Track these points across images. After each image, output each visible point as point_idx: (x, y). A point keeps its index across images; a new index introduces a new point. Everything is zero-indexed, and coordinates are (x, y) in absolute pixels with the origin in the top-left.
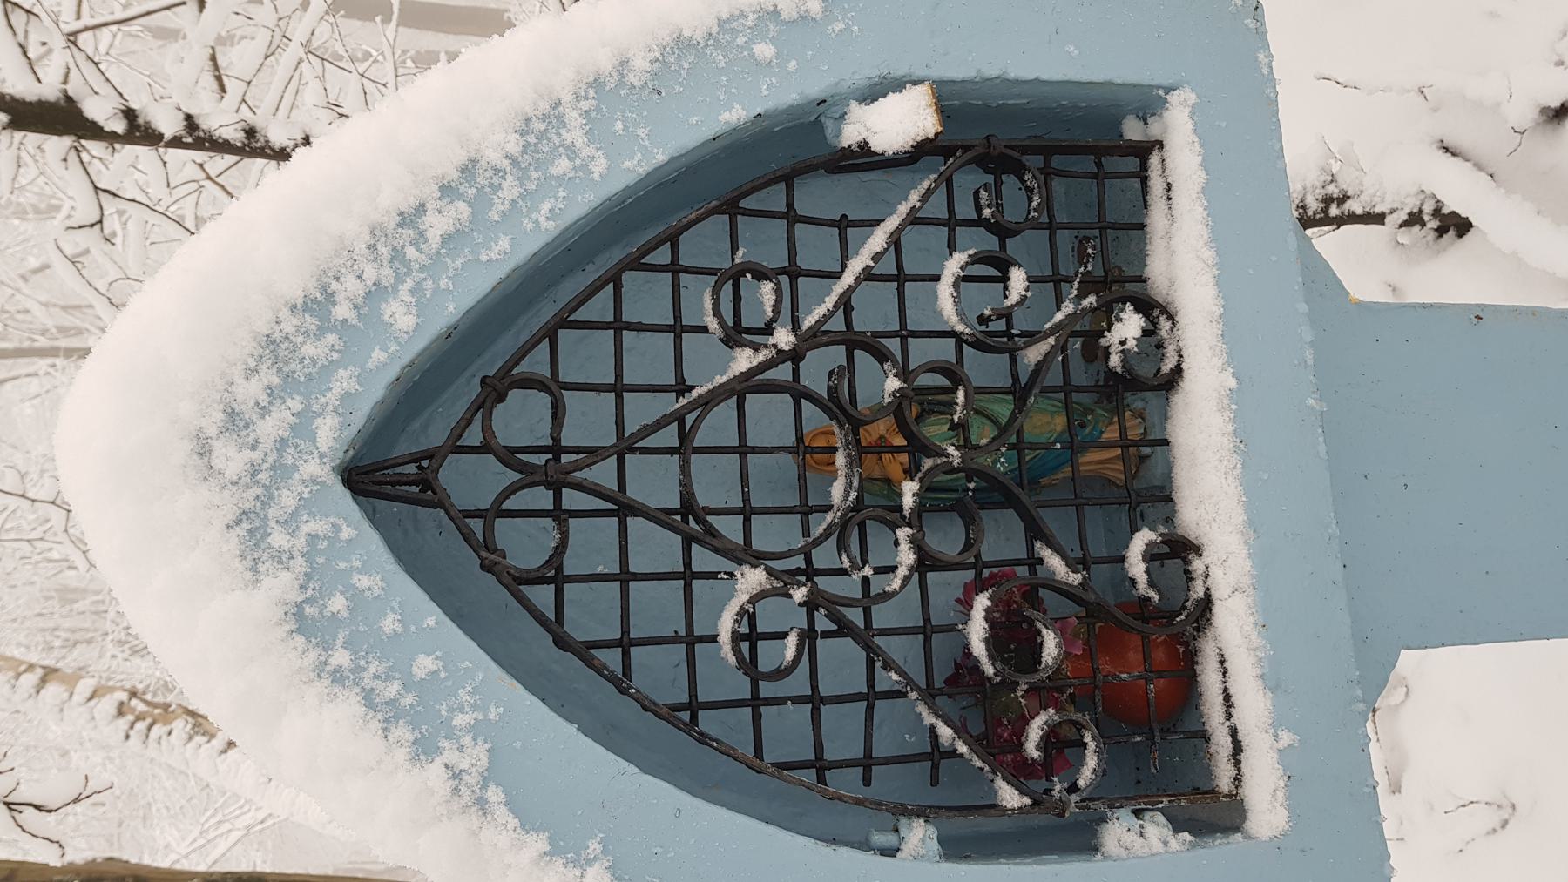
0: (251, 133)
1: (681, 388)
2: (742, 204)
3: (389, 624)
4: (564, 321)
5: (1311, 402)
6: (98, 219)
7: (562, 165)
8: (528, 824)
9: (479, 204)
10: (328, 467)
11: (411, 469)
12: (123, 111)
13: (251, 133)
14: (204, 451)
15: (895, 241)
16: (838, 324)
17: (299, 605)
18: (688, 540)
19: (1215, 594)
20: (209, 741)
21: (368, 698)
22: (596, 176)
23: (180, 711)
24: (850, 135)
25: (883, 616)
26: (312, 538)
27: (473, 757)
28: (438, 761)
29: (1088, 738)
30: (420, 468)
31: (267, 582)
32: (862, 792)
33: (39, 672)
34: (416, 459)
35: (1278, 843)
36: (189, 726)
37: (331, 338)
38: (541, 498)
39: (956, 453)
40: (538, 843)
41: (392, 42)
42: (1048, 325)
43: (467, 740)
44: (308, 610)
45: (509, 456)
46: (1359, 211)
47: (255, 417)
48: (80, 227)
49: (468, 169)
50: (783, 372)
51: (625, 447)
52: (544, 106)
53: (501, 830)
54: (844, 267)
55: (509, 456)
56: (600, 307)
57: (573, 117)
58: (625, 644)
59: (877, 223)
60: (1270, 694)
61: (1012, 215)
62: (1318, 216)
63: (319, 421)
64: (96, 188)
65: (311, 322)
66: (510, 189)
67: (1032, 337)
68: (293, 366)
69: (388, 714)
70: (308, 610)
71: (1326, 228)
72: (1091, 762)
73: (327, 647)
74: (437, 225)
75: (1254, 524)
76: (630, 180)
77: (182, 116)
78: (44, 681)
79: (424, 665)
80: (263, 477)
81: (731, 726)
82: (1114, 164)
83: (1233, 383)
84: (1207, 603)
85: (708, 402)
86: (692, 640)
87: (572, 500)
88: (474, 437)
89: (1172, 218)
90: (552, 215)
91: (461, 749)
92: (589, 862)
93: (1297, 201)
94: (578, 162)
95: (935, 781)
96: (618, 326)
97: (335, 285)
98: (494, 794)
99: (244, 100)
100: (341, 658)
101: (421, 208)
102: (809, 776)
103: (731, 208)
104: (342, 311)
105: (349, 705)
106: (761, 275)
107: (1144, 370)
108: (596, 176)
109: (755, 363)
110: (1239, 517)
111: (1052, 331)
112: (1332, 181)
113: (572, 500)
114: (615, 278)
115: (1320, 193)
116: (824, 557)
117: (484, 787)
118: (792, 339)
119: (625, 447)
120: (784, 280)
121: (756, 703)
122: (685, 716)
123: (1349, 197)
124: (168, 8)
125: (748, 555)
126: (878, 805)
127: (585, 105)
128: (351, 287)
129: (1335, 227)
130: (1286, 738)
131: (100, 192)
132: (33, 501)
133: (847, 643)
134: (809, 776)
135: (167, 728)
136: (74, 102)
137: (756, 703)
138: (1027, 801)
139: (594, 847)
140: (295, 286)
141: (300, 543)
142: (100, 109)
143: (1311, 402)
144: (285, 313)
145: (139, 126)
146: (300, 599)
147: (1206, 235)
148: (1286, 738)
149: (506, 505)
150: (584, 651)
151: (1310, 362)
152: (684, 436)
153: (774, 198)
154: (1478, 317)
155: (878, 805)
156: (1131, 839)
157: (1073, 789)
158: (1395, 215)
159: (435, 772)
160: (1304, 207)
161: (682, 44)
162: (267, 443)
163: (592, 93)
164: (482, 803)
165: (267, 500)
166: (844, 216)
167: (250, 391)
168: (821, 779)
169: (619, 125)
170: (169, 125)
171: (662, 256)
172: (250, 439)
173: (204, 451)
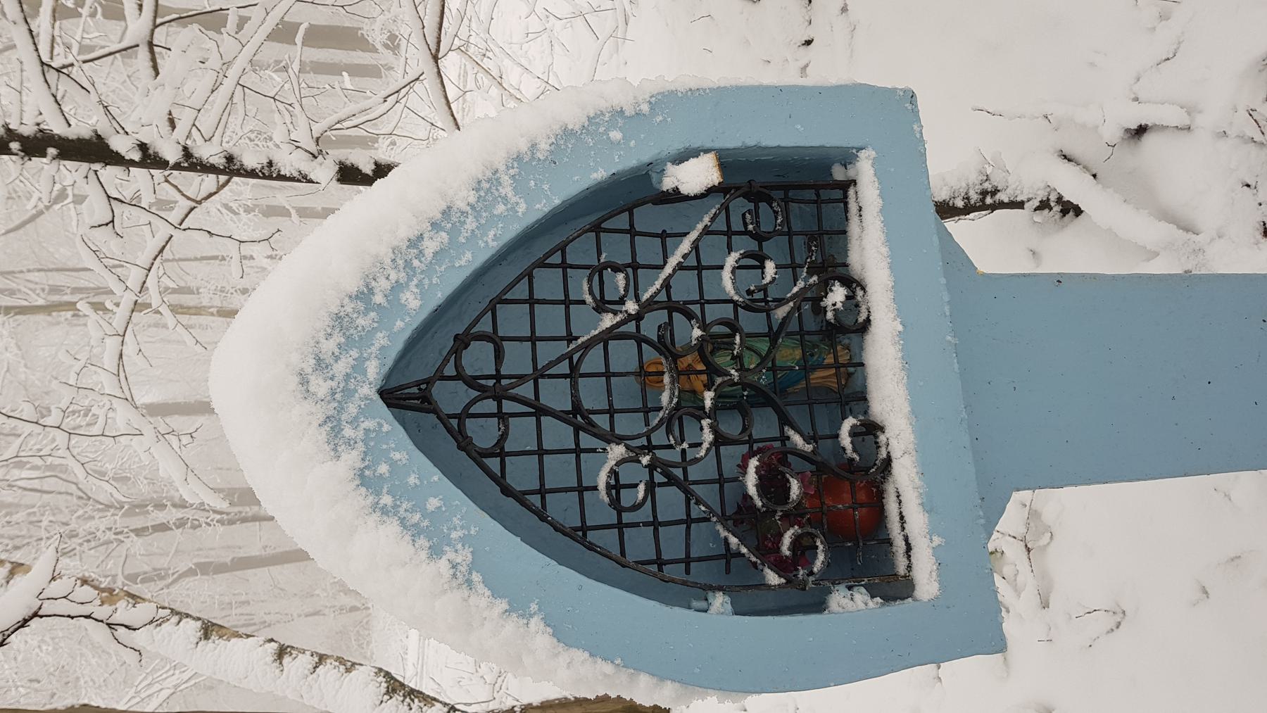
0: (230, 159)
1: (570, 338)
2: (603, 225)
3: (412, 480)
4: (501, 300)
5: (949, 338)
6: (111, 219)
7: (500, 209)
8: (496, 594)
9: (454, 232)
10: (374, 390)
11: (415, 390)
12: (138, 145)
13: (230, 159)
15: (696, 246)
16: (662, 297)
17: (362, 470)
18: (577, 429)
19: (893, 455)
21: (403, 522)
22: (520, 214)
23: (122, 594)
24: (668, 184)
25: (694, 473)
26: (367, 431)
27: (464, 556)
28: (444, 558)
29: (818, 543)
30: (420, 389)
31: (344, 456)
32: (685, 578)
34: (418, 384)
35: (933, 602)
37: (373, 314)
38: (490, 406)
39: (736, 374)
40: (502, 605)
41: (297, 74)
42: (789, 295)
43: (459, 546)
44: (367, 473)
45: (471, 382)
46: (1006, 200)
47: (332, 362)
48: (100, 226)
49: (446, 213)
50: (631, 327)
51: (539, 375)
52: (489, 174)
53: (481, 598)
54: (665, 263)
55: (471, 382)
57: (506, 179)
58: (542, 492)
59: (685, 234)
60: (927, 515)
61: (766, 227)
62: (978, 204)
63: (368, 363)
64: (109, 197)
65: (361, 306)
66: (471, 224)
67: (780, 302)
68: (352, 331)
69: (415, 532)
70: (367, 473)
71: (984, 213)
72: (821, 557)
73: (378, 493)
74: (430, 246)
75: (916, 413)
76: (539, 215)
77: (181, 148)
79: (433, 503)
80: (338, 396)
81: (607, 540)
82: (825, 194)
83: (900, 328)
84: (888, 461)
85: (587, 346)
87: (508, 406)
89: (863, 229)
90: (495, 238)
91: (456, 551)
92: (531, 616)
93: (963, 194)
94: (509, 206)
95: (728, 571)
96: (532, 301)
97: (374, 284)
98: (476, 577)
99: (194, 125)
100: (387, 500)
101: (421, 237)
102: (654, 568)
103: (597, 228)
104: (378, 299)
105: (393, 527)
106: (616, 269)
107: (848, 321)
108: (520, 214)
109: (615, 322)
111: (792, 299)
112: (987, 180)
113: (508, 406)
115: (979, 188)
116: (659, 438)
117: (470, 573)
118: (637, 307)
120: (630, 270)
121: (620, 526)
122: (580, 533)
123: (999, 191)
125: (612, 437)
126: (695, 585)
127: (512, 172)
128: (383, 285)
129: (989, 211)
130: (937, 540)
131: (112, 200)
132: (45, 426)
134: (654, 568)
135: (114, 607)
136: (103, 139)
137: (620, 526)
138: (783, 581)
139: (534, 607)
140: (353, 284)
141: (361, 434)
142: (120, 144)
143: (949, 338)
144: (347, 300)
145: (150, 155)
146: (362, 466)
147: (883, 239)
148: (937, 540)
149: (472, 411)
151: (948, 314)
153: (622, 221)
154: (1059, 281)
155: (695, 585)
156: (846, 602)
157: (811, 573)
158: (1031, 202)
159: (443, 564)
160: (968, 198)
161: (567, 133)
162: (339, 377)
163: (516, 165)
164: (469, 582)
165: (340, 410)
166: (664, 231)
167: (329, 346)
168: (660, 570)
169: (532, 183)
171: (556, 258)
172: (330, 375)
173: (304, 382)
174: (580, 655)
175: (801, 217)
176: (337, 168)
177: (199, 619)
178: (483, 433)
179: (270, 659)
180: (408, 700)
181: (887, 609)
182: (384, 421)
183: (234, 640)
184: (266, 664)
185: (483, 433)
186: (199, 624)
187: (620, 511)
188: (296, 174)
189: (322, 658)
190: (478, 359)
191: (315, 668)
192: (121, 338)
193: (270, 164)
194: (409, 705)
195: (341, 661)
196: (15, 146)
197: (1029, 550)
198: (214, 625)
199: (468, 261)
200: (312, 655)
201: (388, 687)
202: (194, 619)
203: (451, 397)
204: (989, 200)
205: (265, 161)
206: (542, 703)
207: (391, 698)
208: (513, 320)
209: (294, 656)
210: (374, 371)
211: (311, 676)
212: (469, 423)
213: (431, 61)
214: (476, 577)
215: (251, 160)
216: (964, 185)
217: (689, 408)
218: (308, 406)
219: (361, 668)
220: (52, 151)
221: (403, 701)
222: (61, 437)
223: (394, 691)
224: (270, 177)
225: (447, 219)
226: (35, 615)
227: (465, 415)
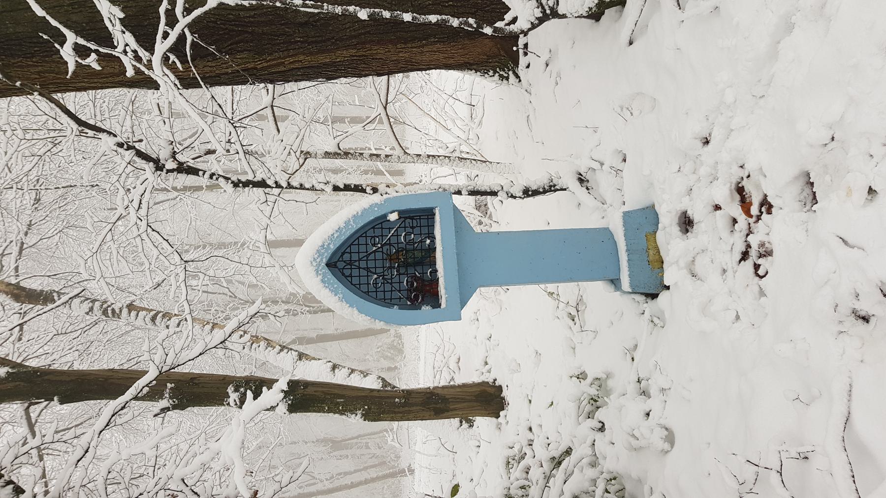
0: (301, 185)
1: (367, 252)
4: (352, 244)
8: (347, 303)
9: (341, 231)
13: (301, 185)
14: (312, 263)
15: (397, 230)
16: (388, 242)
20: (273, 349)
21: (330, 289)
23: (262, 338)
24: (388, 218)
25: (394, 281)
27: (341, 296)
33: (211, 324)
34: (334, 262)
36: (266, 344)
38: (349, 267)
45: (345, 262)
46: (559, 188)
49: (339, 228)
50: (381, 250)
51: (360, 260)
55: (345, 262)
56: (356, 242)
57: (351, 220)
65: (322, 248)
66: (344, 230)
67: (416, 243)
69: (332, 291)
74: (335, 235)
78: (213, 328)
79: (336, 286)
83: (442, 249)
84: (438, 278)
85: (370, 254)
86: (368, 284)
87: (353, 267)
88: (341, 259)
96: (359, 245)
98: (343, 300)
100: (327, 285)
102: (383, 300)
104: (325, 246)
105: (328, 290)
106: (377, 237)
110: (442, 267)
113: (353, 267)
114: (358, 238)
115: (548, 185)
116: (386, 273)
119: (360, 260)
120: (380, 237)
121: (376, 291)
124: (262, 109)
128: (326, 244)
130: (446, 296)
133: (389, 284)
134: (383, 300)
135: (258, 344)
137: (376, 291)
139: (355, 306)
140: (320, 244)
141: (322, 273)
142: (270, 182)
148: (446, 296)
150: (355, 285)
152: (367, 258)
153: (380, 226)
156: (425, 309)
159: (337, 297)
164: (342, 301)
165: (318, 268)
170: (284, 185)
171: (364, 235)
173: (312, 263)
174: (363, 315)
175: (424, 222)
176: (332, 187)
177: (297, 351)
178: (347, 272)
179: (329, 370)
182: (327, 270)
183: (312, 361)
184: (327, 372)
185: (347, 272)
186: (297, 353)
187: (376, 288)
188: (321, 189)
189: (353, 371)
190: (347, 257)
191: (350, 374)
192: (265, 230)
193: (313, 186)
195: (362, 372)
196: (241, 185)
197: (578, 311)
198: (303, 354)
199: (343, 238)
201: (383, 384)
202: (295, 351)
203: (341, 265)
204: (553, 189)
205: (311, 186)
206: (443, 386)
208: (354, 248)
209: (340, 369)
210: (325, 261)
211: (348, 378)
212: (344, 270)
213: (384, 109)
214: (343, 300)
215: (307, 186)
216: (542, 184)
217: (391, 268)
218: (312, 267)
219: (371, 376)
220: (251, 186)
222: (247, 268)
224: (313, 190)
225: (339, 230)
226: (258, 312)
227: (343, 268)
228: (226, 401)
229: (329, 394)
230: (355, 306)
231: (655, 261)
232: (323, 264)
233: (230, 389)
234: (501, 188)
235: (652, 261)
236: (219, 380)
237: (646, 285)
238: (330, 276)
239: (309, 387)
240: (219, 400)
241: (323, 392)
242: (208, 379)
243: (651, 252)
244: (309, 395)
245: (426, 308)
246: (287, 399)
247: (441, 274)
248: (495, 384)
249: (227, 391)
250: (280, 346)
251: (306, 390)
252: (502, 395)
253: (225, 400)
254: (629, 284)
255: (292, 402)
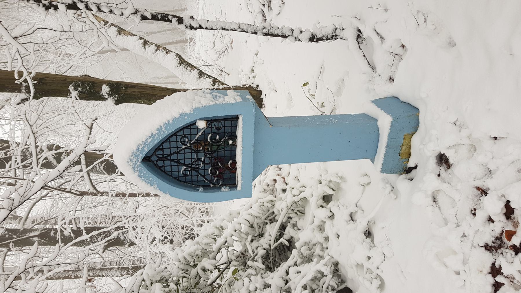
3: (147, 176)
7: (162, 133)
9: (153, 138)
35: (239, 191)
49: (152, 135)
54: (198, 133)
65: (137, 150)
66: (157, 136)
72: (221, 183)
74: (149, 141)
79: (151, 179)
83: (242, 149)
84: (237, 168)
90: (161, 138)
98: (158, 189)
100: (143, 179)
104: (140, 150)
105: (144, 182)
110: (241, 161)
127: (164, 126)
128: (141, 147)
130: (242, 182)
139: (167, 192)
140: (135, 148)
141: (138, 169)
148: (242, 182)
159: (152, 187)
162: (134, 162)
167: (132, 158)
179: (141, 45)
180: (186, 67)
181: (230, 192)
184: (140, 47)
191: (156, 51)
194: (187, 68)
195: (165, 49)
200: (155, 46)
207: (181, 65)
209: (149, 45)
221: (185, 67)
223: (182, 63)
228: (69, 96)
229: (143, 94)
230: (167, 192)
231: (405, 153)
232: (138, 163)
233: (71, 88)
234: (291, 34)
235: (402, 154)
236: (62, 81)
237: (392, 169)
238: (146, 172)
239: (129, 88)
240: (64, 94)
241: (139, 92)
242: (53, 79)
243: (404, 147)
244: (129, 94)
245: (225, 189)
246: (114, 97)
247: (239, 165)
248: (257, 89)
249: (69, 89)
250: (104, 21)
251: (127, 90)
252: (261, 97)
253: (68, 94)
254: (381, 169)
255: (117, 99)
